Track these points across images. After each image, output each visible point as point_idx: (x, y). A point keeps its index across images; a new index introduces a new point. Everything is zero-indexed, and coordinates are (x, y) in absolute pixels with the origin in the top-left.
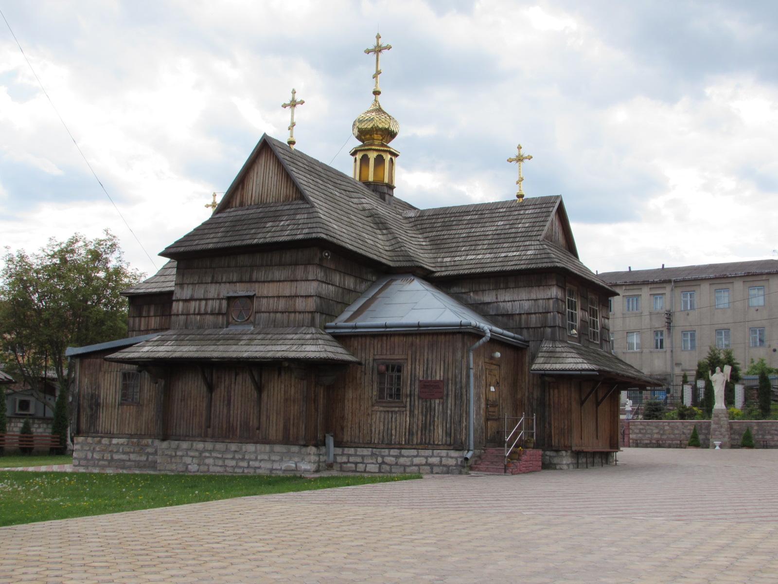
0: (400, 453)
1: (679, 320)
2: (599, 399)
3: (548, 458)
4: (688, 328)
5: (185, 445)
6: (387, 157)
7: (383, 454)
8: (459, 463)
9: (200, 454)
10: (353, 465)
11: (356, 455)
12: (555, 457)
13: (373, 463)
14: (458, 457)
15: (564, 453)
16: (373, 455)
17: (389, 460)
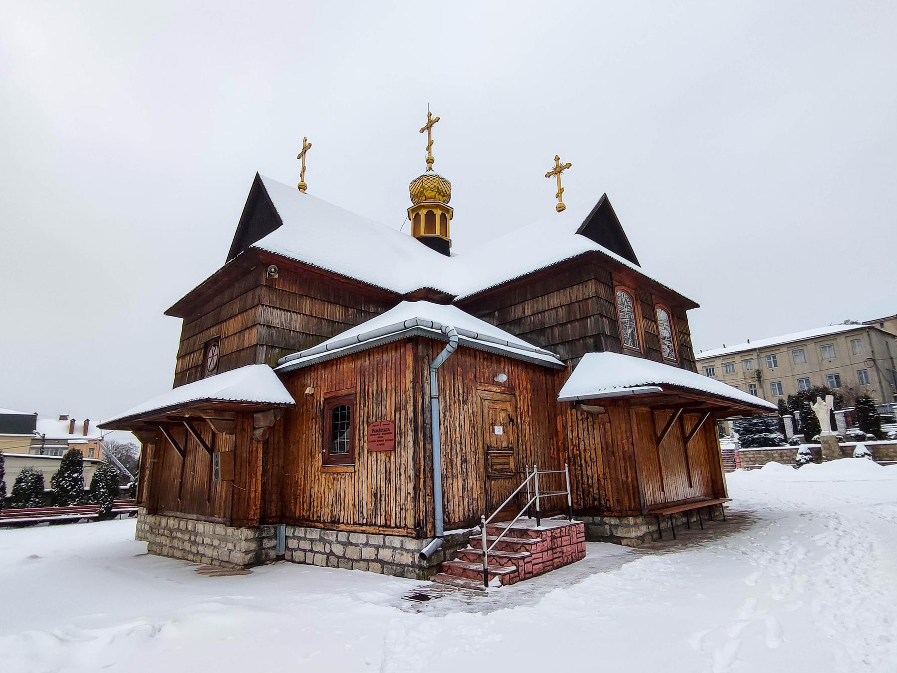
0: (348, 539)
1: (767, 375)
2: (688, 432)
3: (607, 527)
4: (776, 380)
5: (164, 521)
6: (438, 213)
7: (331, 538)
8: (417, 563)
9: (171, 533)
10: (302, 554)
11: (305, 539)
12: (618, 526)
13: (321, 553)
14: (415, 551)
15: (631, 520)
16: (321, 539)
17: (338, 550)
